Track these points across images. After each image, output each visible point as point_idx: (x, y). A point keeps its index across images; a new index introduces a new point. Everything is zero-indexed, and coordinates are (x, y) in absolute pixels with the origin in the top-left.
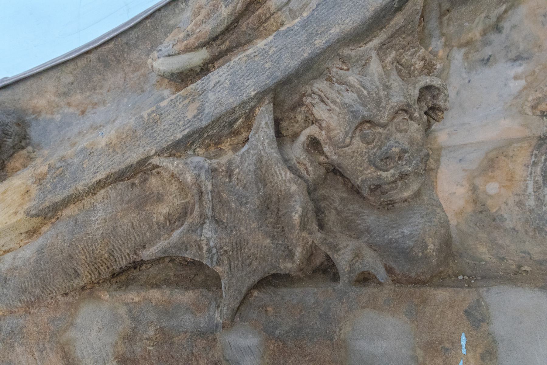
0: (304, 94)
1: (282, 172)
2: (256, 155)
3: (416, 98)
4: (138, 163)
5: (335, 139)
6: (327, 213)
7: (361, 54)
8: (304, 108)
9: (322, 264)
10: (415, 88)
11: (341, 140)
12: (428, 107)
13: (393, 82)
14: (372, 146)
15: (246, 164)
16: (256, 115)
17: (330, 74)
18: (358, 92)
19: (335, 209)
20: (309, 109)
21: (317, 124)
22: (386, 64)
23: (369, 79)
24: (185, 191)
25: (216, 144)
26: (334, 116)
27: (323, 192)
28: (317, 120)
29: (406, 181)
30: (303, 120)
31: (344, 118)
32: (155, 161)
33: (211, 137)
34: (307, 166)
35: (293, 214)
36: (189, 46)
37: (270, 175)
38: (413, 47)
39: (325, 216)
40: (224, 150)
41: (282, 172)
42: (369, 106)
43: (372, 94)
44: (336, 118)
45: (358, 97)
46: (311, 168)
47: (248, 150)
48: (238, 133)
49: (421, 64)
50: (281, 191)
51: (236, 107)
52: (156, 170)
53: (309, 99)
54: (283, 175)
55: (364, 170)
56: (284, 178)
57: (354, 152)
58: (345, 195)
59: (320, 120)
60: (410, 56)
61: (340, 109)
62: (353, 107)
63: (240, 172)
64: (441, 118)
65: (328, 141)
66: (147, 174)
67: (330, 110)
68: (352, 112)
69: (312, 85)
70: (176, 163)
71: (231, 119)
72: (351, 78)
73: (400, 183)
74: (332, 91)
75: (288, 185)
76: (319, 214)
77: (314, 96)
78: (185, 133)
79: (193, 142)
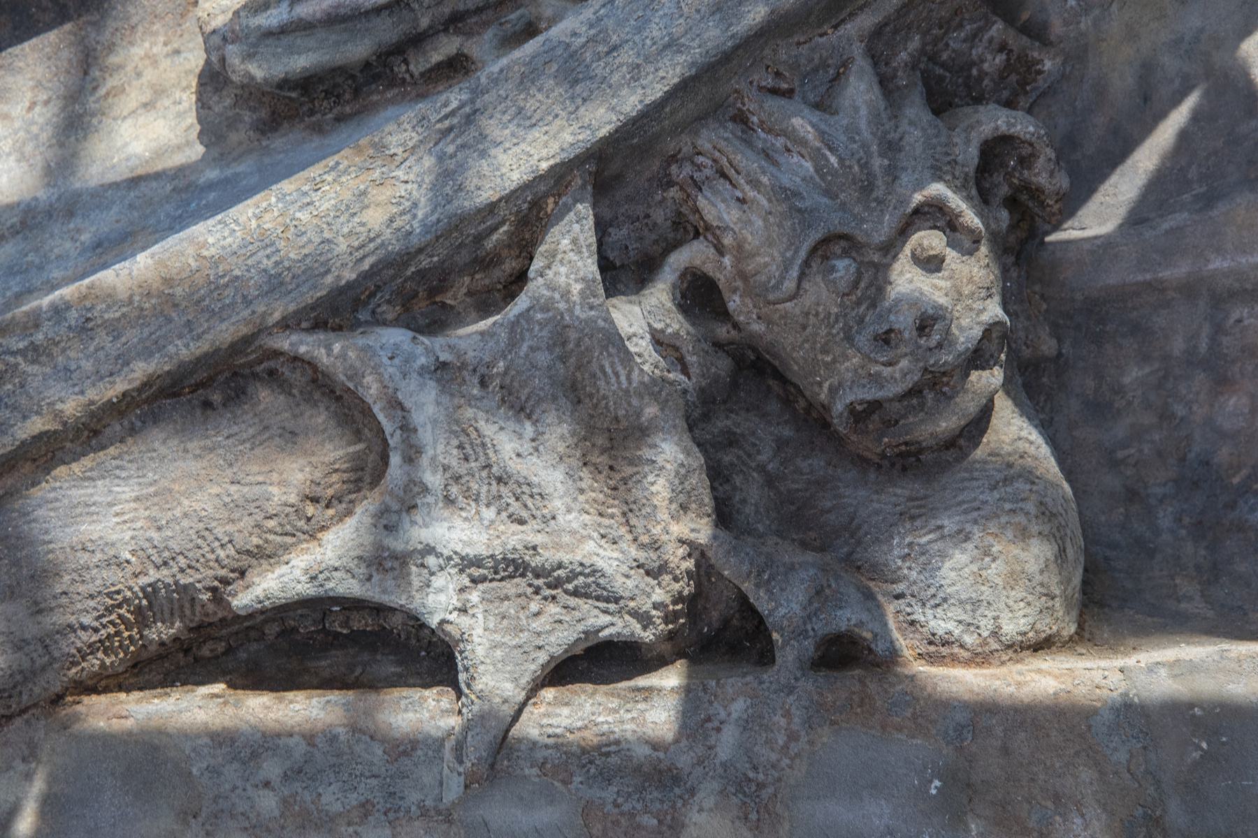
0: (673, 156)
1: (619, 368)
2: (549, 327)
3: (971, 169)
4: (233, 345)
5: (758, 278)
6: (738, 480)
7: (825, 54)
8: (673, 192)
9: (726, 622)
10: (968, 142)
11: (773, 282)
12: (1011, 185)
13: (907, 128)
14: (854, 298)
15: (525, 348)
16: (548, 216)
17: (744, 104)
18: (817, 157)
19: (761, 468)
20: (688, 196)
21: (710, 237)
22: (895, 70)
23: (845, 122)
24: (354, 422)
25: (433, 292)
26: (754, 218)
27: (729, 423)
28: (708, 228)
29: (945, 389)
30: (669, 223)
31: (780, 226)
32: (285, 343)
33: (421, 274)
34: (684, 350)
35: (651, 478)
36: (342, 11)
37: (587, 376)
38: (972, 21)
39: (735, 488)
40: (452, 307)
41: (619, 368)
42: (842, 196)
43: (850, 167)
44: (760, 223)
45: (817, 171)
46: (694, 358)
47: (528, 310)
48: (492, 259)
49: (997, 61)
50: (617, 419)
51: (500, 200)
52: (265, 365)
53: (687, 169)
54: (623, 378)
55: (834, 361)
56: (625, 385)
57: (807, 314)
58: (787, 432)
59: (719, 228)
60: (965, 41)
61: (770, 201)
62: (803, 198)
63: (507, 370)
64: (1054, 214)
65: (739, 283)
66: (243, 376)
67: (742, 201)
68: (799, 211)
69: (697, 133)
70: (337, 347)
71: (483, 226)
72: (797, 122)
73: (929, 396)
74: (749, 152)
75: (635, 402)
76: (716, 484)
77: (701, 159)
78: (366, 265)
79: (378, 288)
